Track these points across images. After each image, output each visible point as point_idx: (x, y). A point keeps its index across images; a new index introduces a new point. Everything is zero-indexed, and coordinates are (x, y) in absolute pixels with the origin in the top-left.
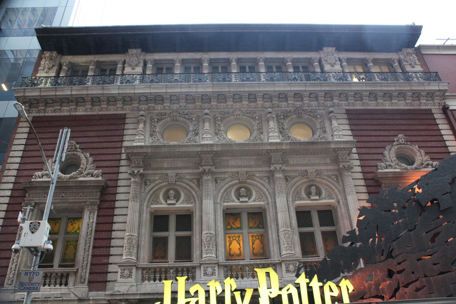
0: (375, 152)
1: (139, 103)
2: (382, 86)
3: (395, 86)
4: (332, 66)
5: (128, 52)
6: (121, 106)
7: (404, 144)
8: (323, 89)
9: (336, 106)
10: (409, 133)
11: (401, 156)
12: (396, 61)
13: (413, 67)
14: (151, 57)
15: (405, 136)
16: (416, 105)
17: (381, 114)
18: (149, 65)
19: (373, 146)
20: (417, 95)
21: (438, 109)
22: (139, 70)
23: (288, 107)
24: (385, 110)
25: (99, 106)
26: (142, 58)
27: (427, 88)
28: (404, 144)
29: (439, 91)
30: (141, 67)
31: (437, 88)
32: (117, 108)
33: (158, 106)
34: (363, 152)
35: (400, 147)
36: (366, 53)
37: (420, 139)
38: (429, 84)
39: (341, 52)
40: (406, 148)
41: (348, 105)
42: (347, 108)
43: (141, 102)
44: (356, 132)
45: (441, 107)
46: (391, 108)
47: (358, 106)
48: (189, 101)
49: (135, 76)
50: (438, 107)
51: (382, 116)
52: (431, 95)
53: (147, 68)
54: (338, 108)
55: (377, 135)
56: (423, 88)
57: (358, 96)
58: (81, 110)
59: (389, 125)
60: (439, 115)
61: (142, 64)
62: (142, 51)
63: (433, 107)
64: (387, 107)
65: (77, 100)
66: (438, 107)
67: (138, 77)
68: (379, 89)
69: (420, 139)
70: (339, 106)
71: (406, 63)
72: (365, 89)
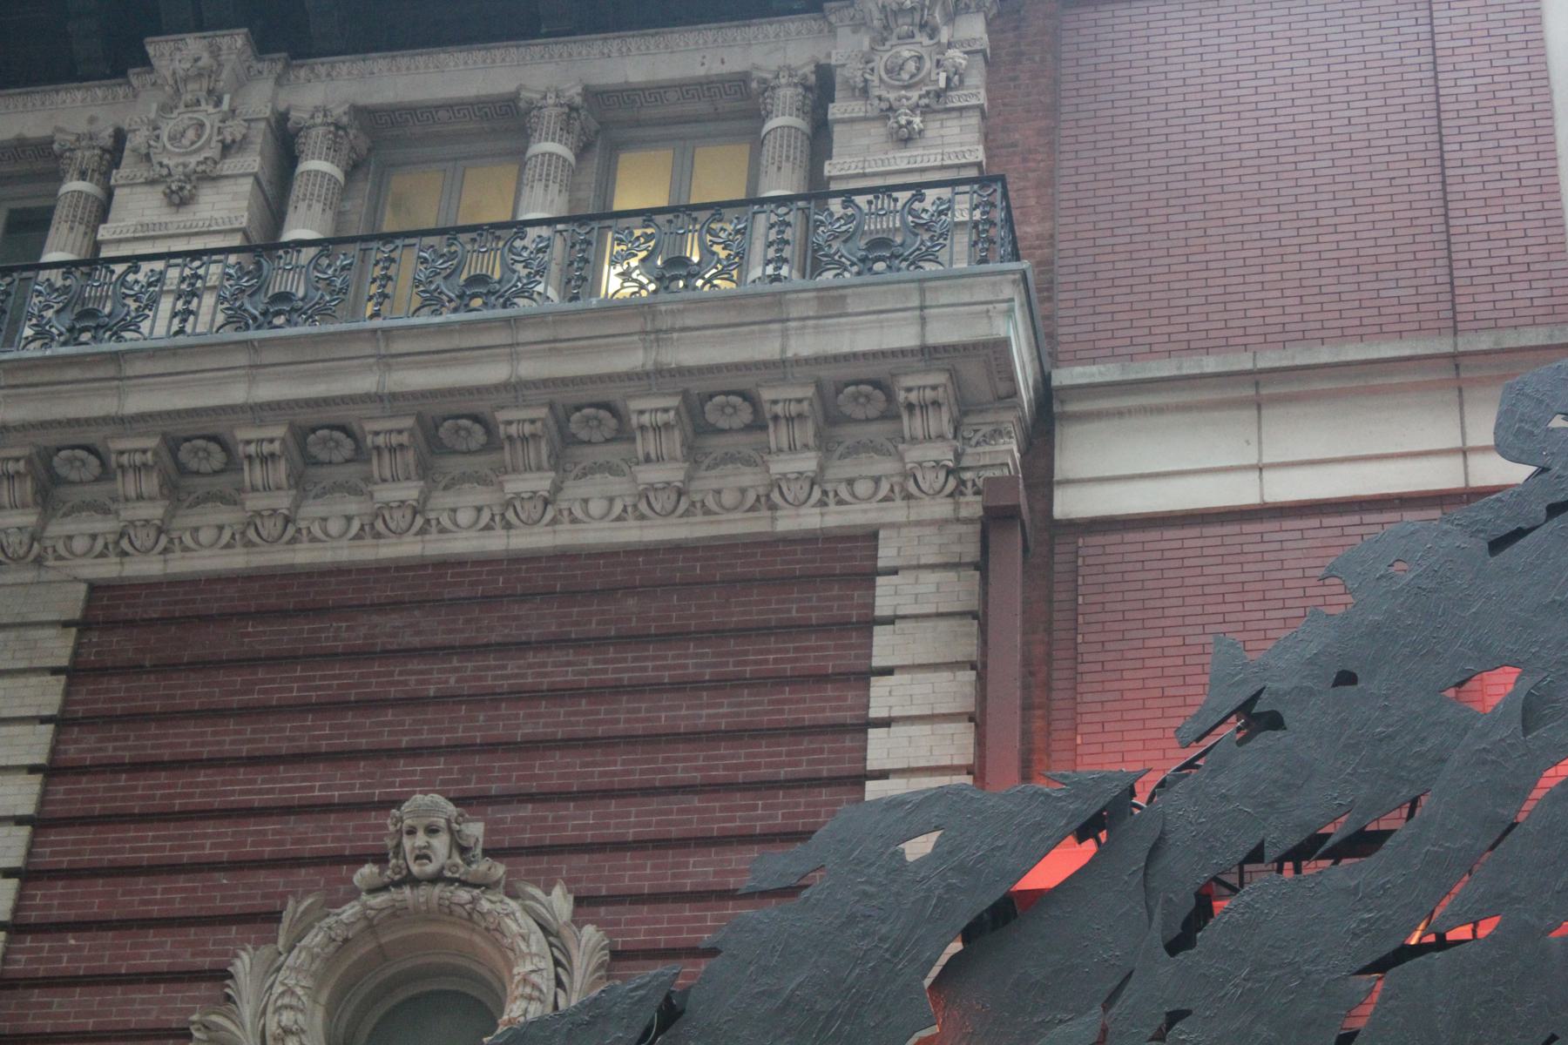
0: (163, 963)
1: (425, 471)
2: (387, 361)
3: (513, 351)
4: (180, 199)
5: (145, 62)
6: (155, 511)
7: (436, 879)
8: (137, 403)
9: (17, 560)
10: (502, 775)
11: (401, 995)
12: (787, 94)
13: (906, 139)
14: (330, 89)
15: (457, 801)
16: (728, 499)
17: (396, 605)
18: (317, 165)
19: (178, 907)
20: (718, 413)
21: (942, 523)
22: (227, 207)
23: (508, 526)
24: (443, 565)
25: (355, 491)
26: (260, 99)
27: (804, 345)
28: (436, 879)
29: (928, 353)
30: (247, 185)
31: (905, 337)
32: (509, 504)
33: (449, 500)
34: (65, 964)
35: (397, 914)
36: (536, 49)
37: (578, 822)
38: (831, 303)
39: (321, 66)
40: (447, 911)
41: (119, 545)
42: (108, 569)
43: (63, 492)
44: (85, 782)
45: (972, 506)
46: (496, 543)
47: (209, 549)
48: (851, 433)
49: (145, 267)
50: (942, 508)
51: (395, 620)
52: (857, 400)
53: (298, 189)
54: (29, 575)
55: (256, 800)
56: (767, 348)
57: (194, 457)
58: (206, 536)
59: (414, 702)
60: (930, 579)
61: (252, 161)
62: (263, 45)
63: (898, 512)
64: (464, 544)
65: (49, 468)
66: (942, 508)
67: (174, 274)
68: (365, 383)
69: (578, 822)
70: (39, 561)
71: (857, 108)
72: (237, 394)
